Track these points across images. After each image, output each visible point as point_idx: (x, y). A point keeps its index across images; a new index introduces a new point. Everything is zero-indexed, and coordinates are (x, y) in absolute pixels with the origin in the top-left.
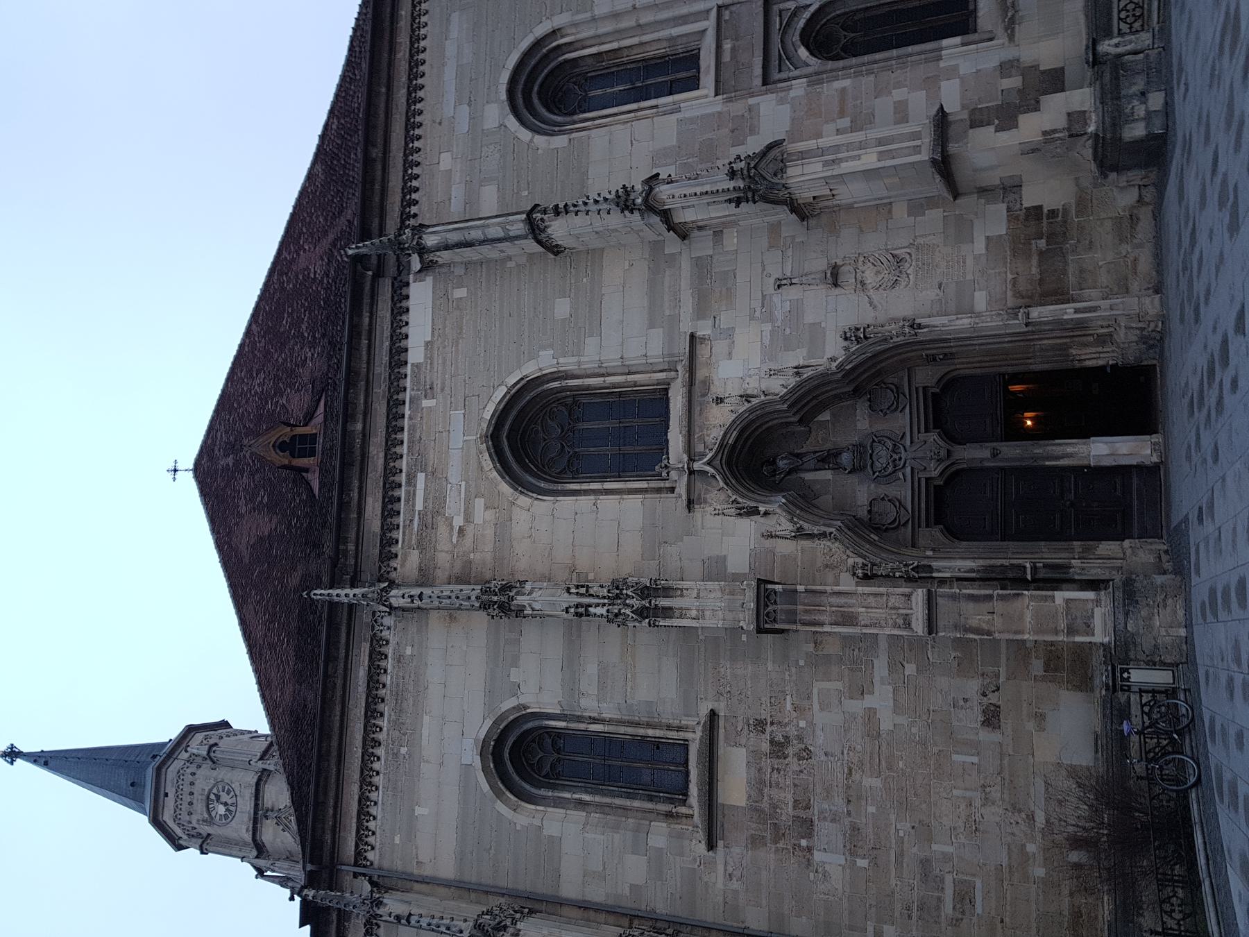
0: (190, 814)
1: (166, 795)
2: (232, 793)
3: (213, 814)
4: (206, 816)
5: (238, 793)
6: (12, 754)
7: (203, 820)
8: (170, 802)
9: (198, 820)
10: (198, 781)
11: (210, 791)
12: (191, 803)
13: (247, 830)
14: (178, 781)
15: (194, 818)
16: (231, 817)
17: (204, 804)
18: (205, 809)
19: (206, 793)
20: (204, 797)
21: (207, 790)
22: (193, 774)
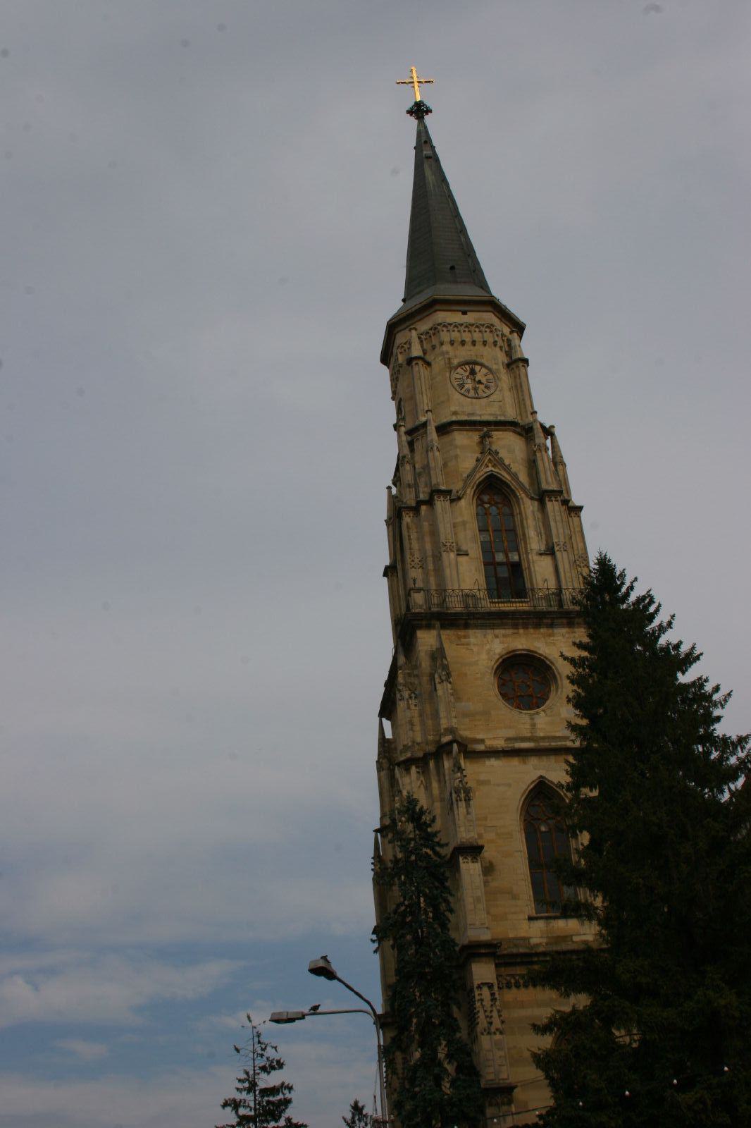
0: (452, 343)
1: (464, 313)
2: (488, 392)
3: (459, 370)
4: (455, 362)
5: (492, 398)
6: (419, 111)
7: (449, 359)
8: (456, 318)
9: (447, 353)
10: (490, 350)
11: (482, 365)
12: (463, 343)
13: (455, 413)
14: (483, 325)
15: (446, 348)
16: (462, 391)
17: (468, 358)
18: (462, 360)
19: (479, 360)
20: (474, 358)
21: (484, 361)
22: (495, 343)
